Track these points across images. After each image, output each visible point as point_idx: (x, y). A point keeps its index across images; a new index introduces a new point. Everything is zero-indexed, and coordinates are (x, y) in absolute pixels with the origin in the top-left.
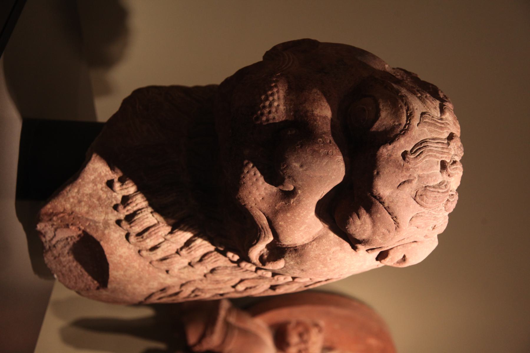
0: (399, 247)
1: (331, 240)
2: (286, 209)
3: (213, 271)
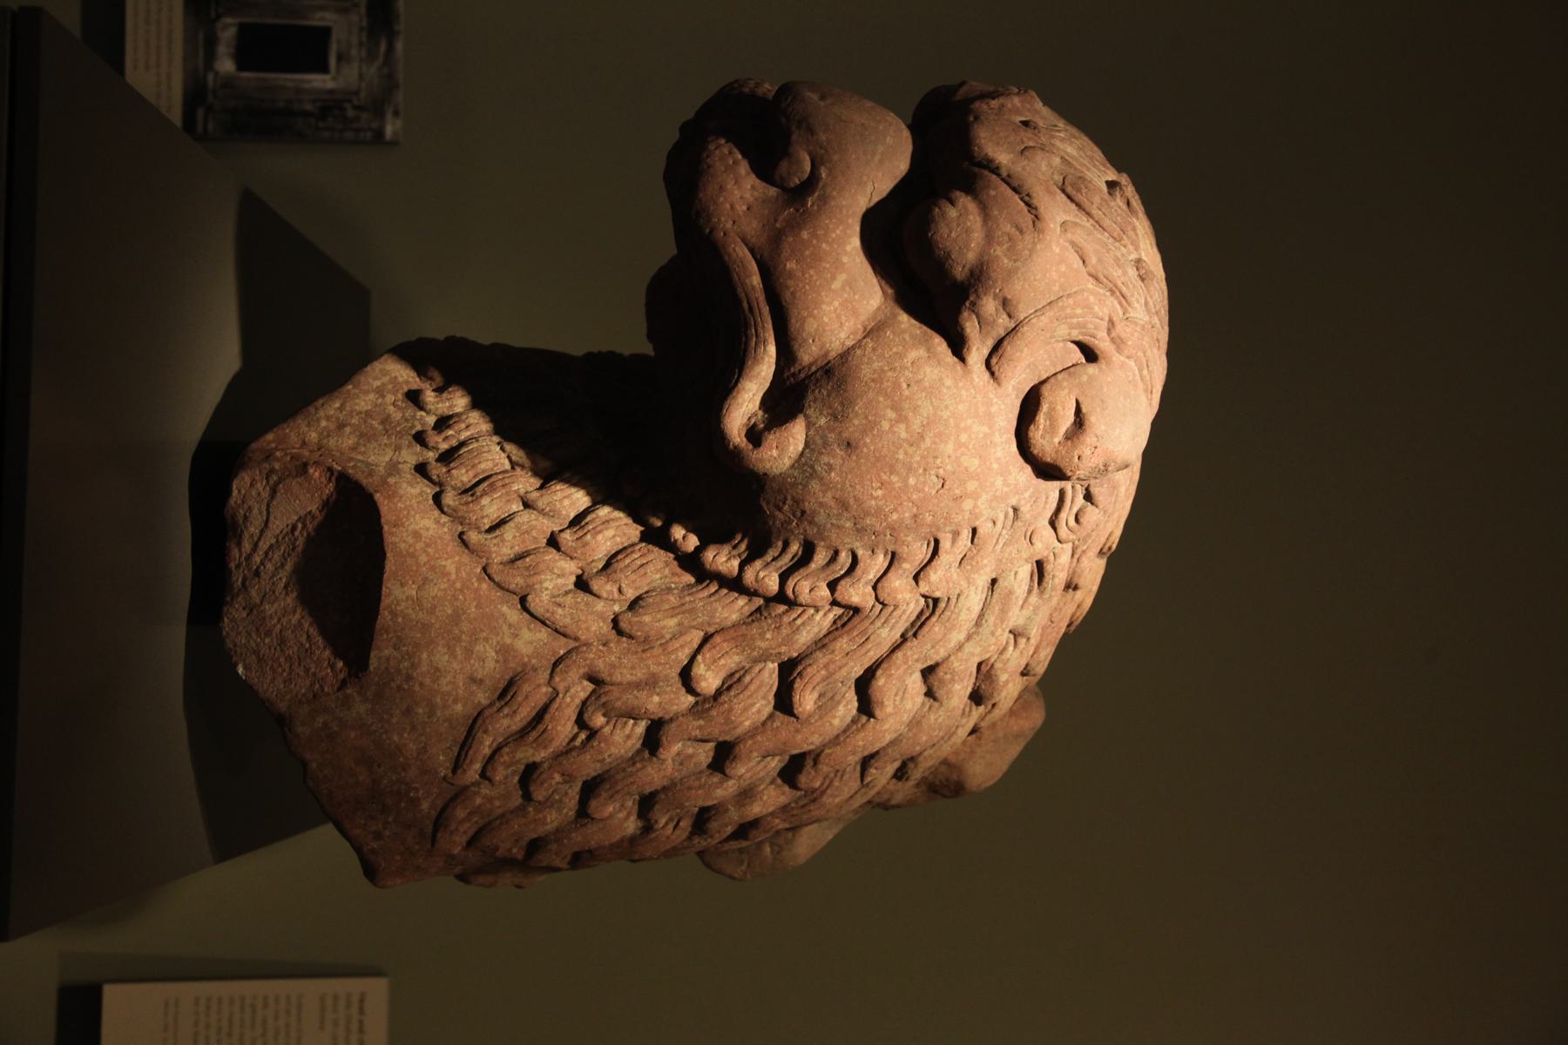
0: (1060, 377)
1: (904, 332)
2: (801, 219)
3: (634, 605)
